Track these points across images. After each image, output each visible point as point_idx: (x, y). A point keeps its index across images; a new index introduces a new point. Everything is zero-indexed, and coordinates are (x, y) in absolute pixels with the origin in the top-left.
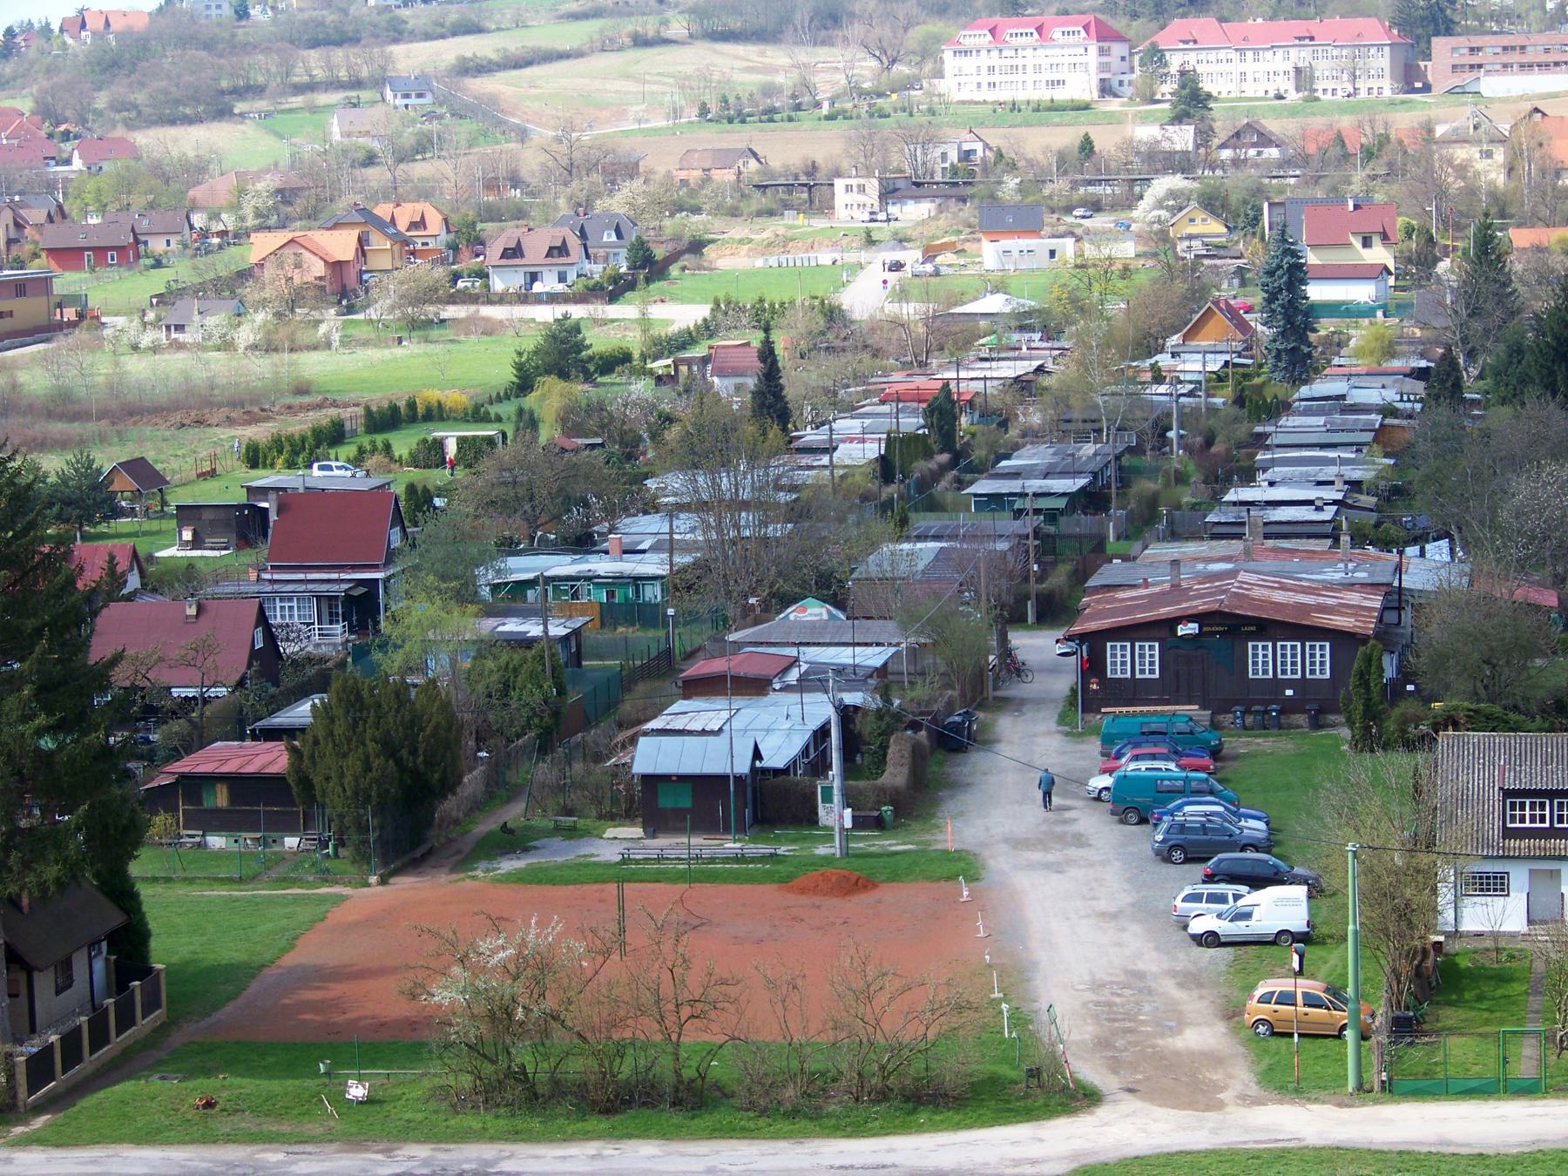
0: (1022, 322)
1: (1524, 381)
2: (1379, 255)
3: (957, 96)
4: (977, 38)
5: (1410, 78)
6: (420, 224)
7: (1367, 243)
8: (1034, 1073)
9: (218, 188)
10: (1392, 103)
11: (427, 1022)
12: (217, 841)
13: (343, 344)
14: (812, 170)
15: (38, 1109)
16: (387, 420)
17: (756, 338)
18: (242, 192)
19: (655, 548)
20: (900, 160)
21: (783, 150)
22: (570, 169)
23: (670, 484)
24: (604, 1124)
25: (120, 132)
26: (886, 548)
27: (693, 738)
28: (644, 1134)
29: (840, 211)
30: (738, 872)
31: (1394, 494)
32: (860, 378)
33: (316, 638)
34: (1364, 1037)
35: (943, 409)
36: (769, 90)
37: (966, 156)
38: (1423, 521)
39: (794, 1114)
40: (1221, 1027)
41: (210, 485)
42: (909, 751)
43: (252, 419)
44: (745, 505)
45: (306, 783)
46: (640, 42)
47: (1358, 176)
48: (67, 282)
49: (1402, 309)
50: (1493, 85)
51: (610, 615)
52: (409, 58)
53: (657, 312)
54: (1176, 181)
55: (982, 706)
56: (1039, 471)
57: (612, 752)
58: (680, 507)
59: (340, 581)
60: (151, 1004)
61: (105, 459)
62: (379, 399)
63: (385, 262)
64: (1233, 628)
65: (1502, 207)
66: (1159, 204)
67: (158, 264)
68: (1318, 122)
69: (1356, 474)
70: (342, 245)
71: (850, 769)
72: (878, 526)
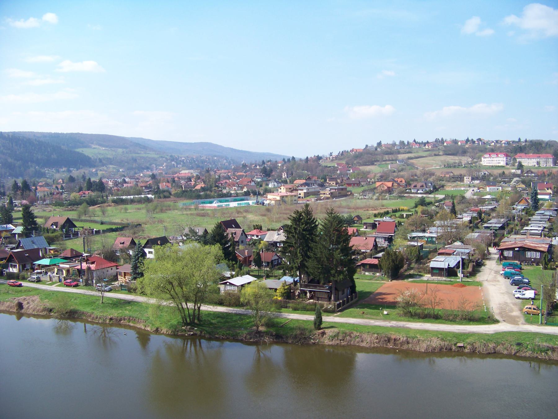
0: (493, 200)
3: (485, 164)
6: (401, 182)
7: (548, 189)
8: (489, 317)
9: (372, 175)
10: (552, 167)
11: (397, 302)
12: (367, 273)
13: (390, 199)
14: (461, 175)
15: (339, 311)
16: (395, 211)
17: (452, 201)
18: (375, 176)
20: (475, 174)
21: (457, 172)
22: (424, 174)
23: (437, 223)
24: (422, 320)
25: (358, 167)
28: (428, 322)
29: (465, 182)
31: (551, 229)
32: (467, 207)
33: (382, 243)
34: (542, 315)
35: (480, 213)
36: (455, 163)
37: (485, 174)
38: (555, 234)
39: (451, 321)
40: (519, 312)
41: (369, 220)
42: (472, 266)
43: (375, 210)
44: (449, 227)
45: (380, 265)
46: (435, 155)
47: (547, 179)
48: (349, 188)
49: (553, 200)
51: (427, 242)
52: (401, 157)
53: (437, 196)
54: (518, 179)
55: (484, 259)
56: (495, 223)
57: (427, 263)
59: (387, 235)
60: (356, 297)
61: (353, 215)
62: (394, 208)
63: (396, 187)
64: (524, 249)
66: (515, 182)
67: (362, 186)
68: (540, 170)
69: (545, 226)
70: (390, 184)
71: (463, 268)
72: (469, 230)
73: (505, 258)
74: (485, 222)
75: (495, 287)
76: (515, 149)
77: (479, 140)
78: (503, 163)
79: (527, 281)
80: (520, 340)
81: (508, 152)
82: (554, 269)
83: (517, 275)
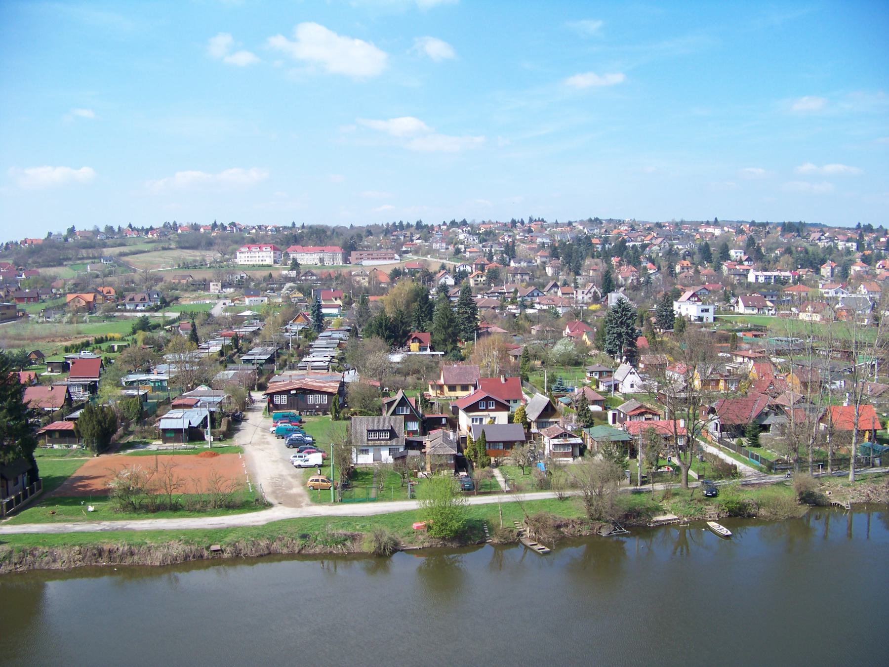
0: (255, 317)
1: (372, 332)
2: (339, 302)
4: (245, 249)
5: (346, 260)
6: (109, 292)
8: (257, 500)
9: (59, 283)
11: (109, 489)
12: (56, 446)
13: (90, 321)
14: (205, 280)
15: (9, 515)
16: (100, 341)
17: (191, 321)
18: (65, 284)
19: (166, 372)
20: (227, 278)
21: (199, 275)
22: (146, 279)
23: (169, 357)
24: (153, 515)
25: (35, 269)
26: (222, 372)
27: (174, 420)
28: (162, 517)
29: (212, 290)
30: (186, 452)
31: (342, 359)
32: (216, 331)
34: (335, 489)
35: (236, 339)
36: (195, 261)
37: (242, 277)
38: (349, 365)
39: (199, 511)
40: (302, 488)
41: (56, 357)
42: (227, 422)
43: (66, 340)
45: (78, 431)
46: (164, 249)
48: (20, 305)
49: (344, 315)
50: (365, 263)
51: (154, 389)
52: (108, 252)
53: (167, 314)
54: (292, 284)
56: (259, 353)
57: (155, 423)
58: (172, 362)
59: (87, 381)
60: (39, 488)
61: (29, 350)
62: (98, 336)
63: (100, 302)
64: (304, 392)
65: (367, 291)
67: (44, 301)
68: (325, 271)
70: (90, 297)
71: (213, 427)
72: (220, 367)
73: (277, 407)
74: (245, 353)
75: (263, 453)
76: (288, 239)
77: (233, 224)
78: (269, 261)
79: (310, 439)
80: (305, 530)
81: (277, 243)
82: (349, 418)
83: (296, 431)
